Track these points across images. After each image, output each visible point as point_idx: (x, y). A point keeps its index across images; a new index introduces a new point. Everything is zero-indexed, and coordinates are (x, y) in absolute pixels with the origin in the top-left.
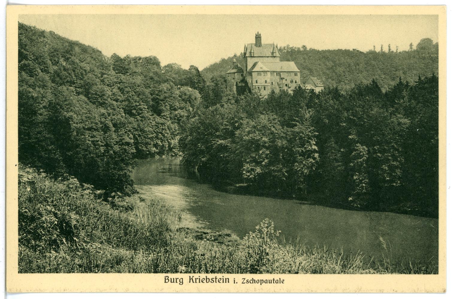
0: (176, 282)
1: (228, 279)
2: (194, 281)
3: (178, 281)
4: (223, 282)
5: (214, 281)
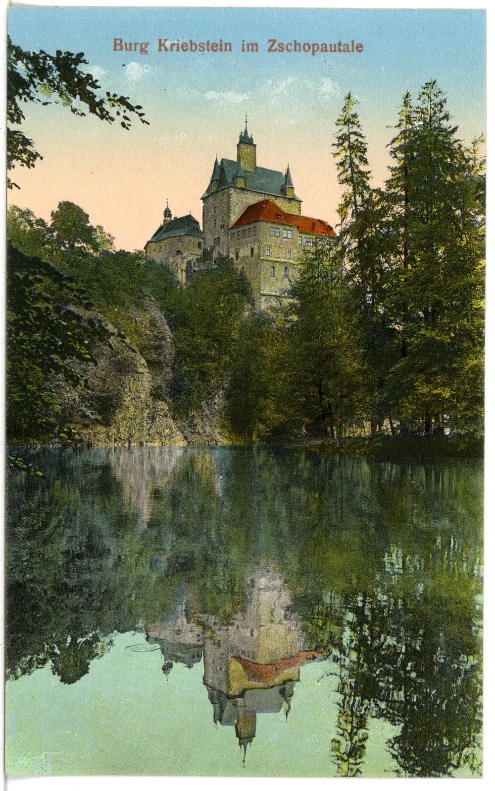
1: (230, 44)
4: (221, 50)
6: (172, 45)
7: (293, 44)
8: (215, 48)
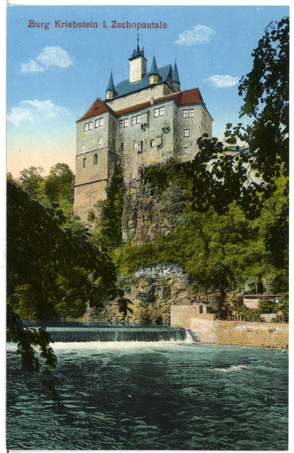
1: (97, 23)
2: (61, 25)
3: (43, 25)
5: (81, 26)
6: (63, 24)
7: (126, 23)
8: (88, 26)
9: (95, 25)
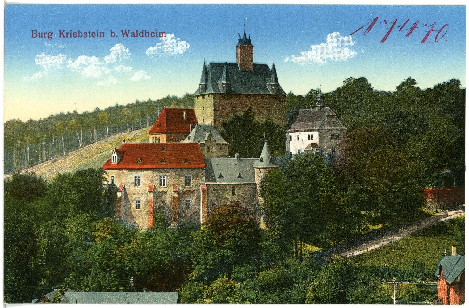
0: (45, 37)
1: (103, 33)
2: (65, 36)
3: (47, 35)
6: (67, 33)
9: (102, 34)
